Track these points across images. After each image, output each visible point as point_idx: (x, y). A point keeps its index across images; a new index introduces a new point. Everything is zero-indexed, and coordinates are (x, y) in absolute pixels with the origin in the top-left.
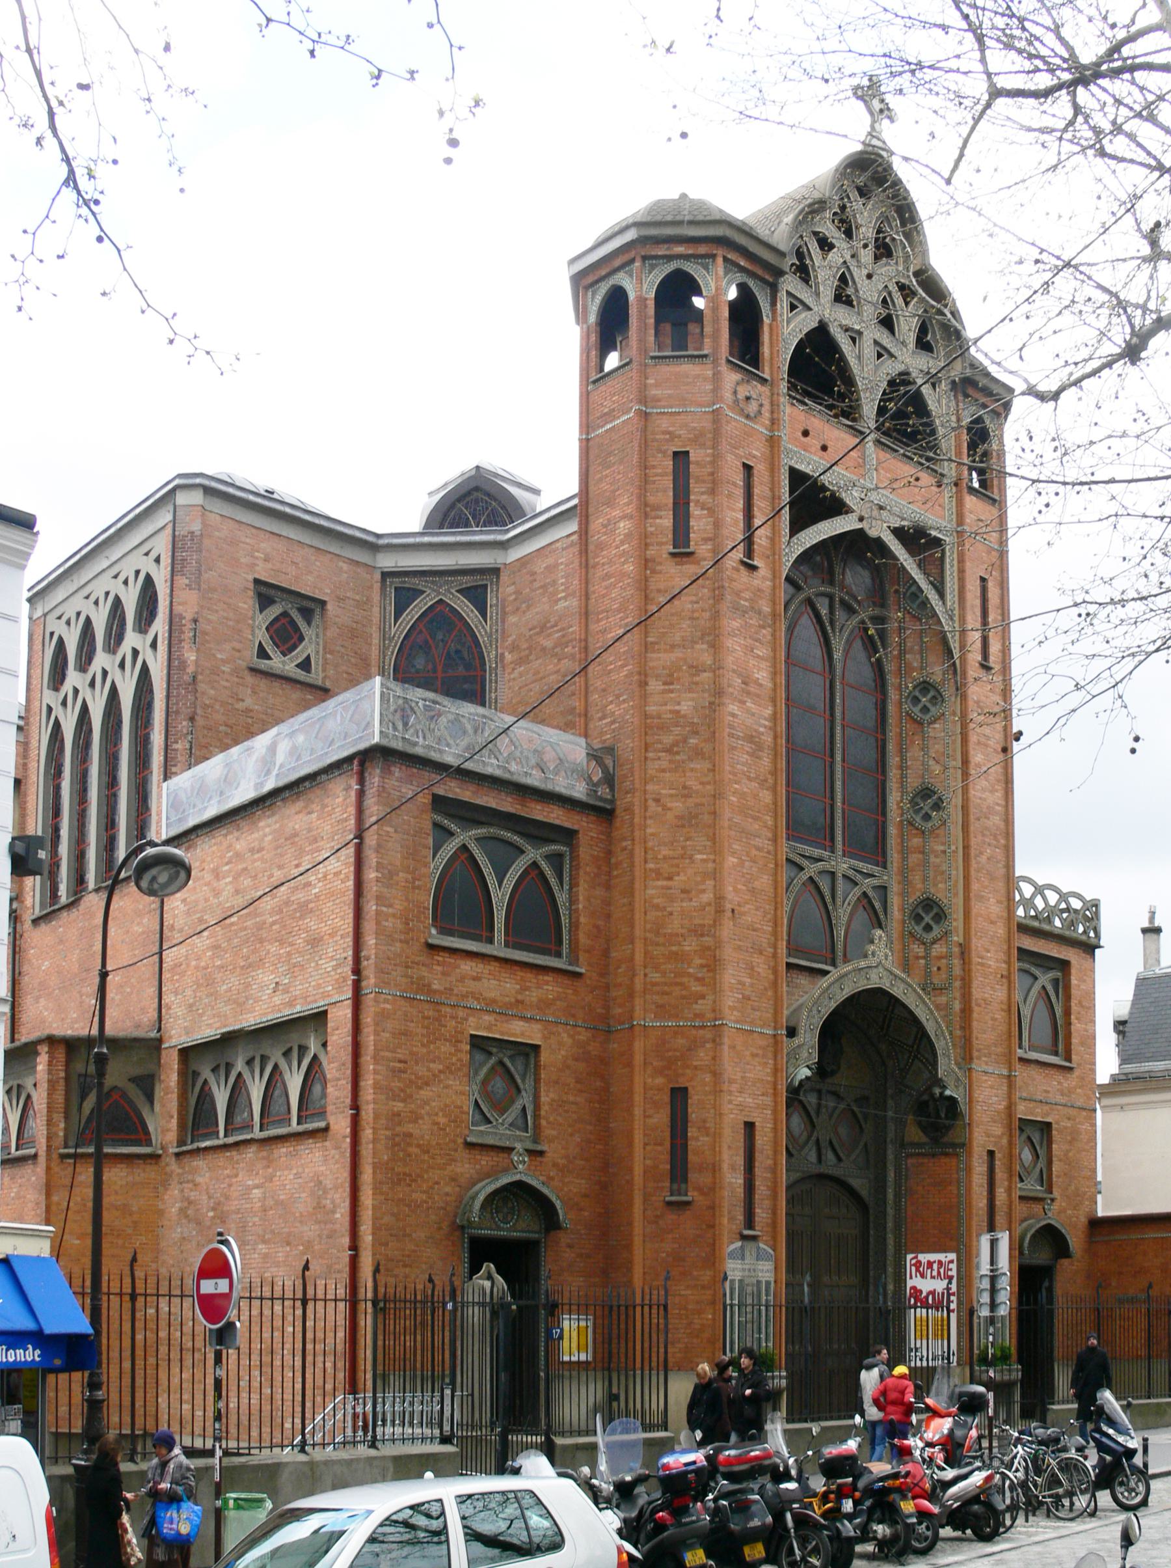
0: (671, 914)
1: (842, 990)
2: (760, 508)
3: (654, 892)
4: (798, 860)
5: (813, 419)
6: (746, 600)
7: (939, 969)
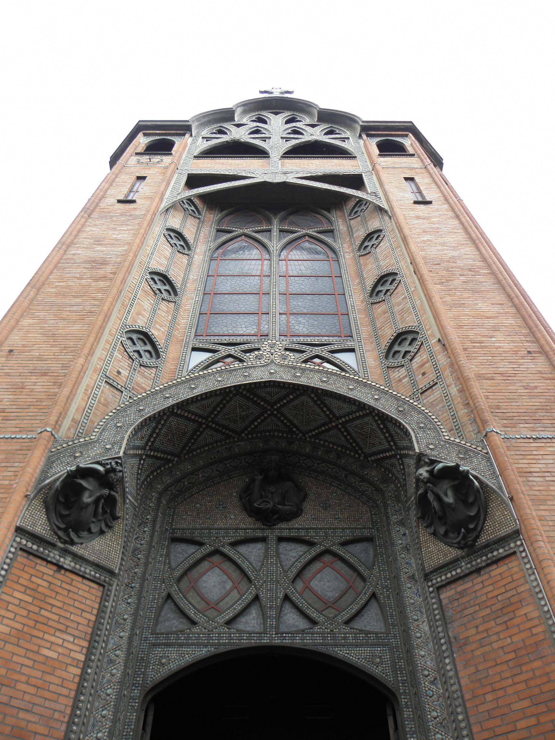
4: (210, 347)
7: (424, 374)
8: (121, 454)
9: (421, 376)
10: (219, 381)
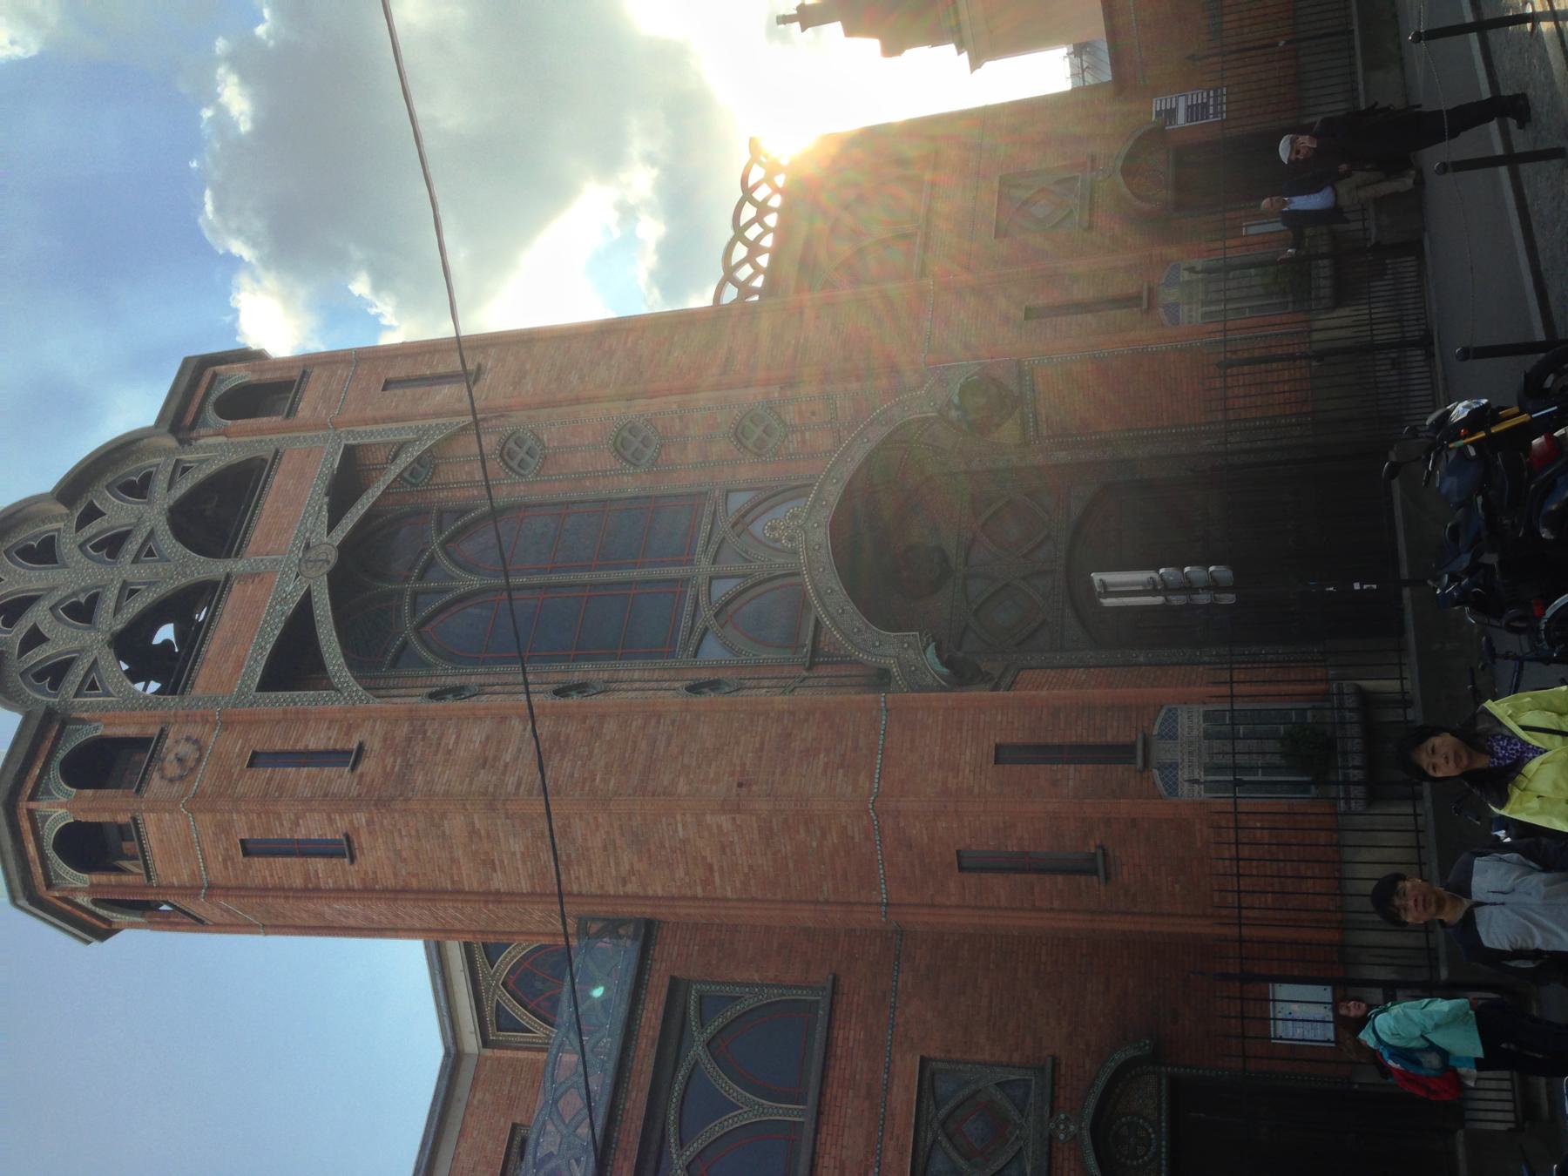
0: (750, 867)
1: (832, 591)
2: (297, 741)
3: (729, 888)
4: (695, 638)
5: (209, 655)
6: (395, 762)
7: (813, 414)
8: (917, 633)
9: (814, 418)
10: (824, 570)
